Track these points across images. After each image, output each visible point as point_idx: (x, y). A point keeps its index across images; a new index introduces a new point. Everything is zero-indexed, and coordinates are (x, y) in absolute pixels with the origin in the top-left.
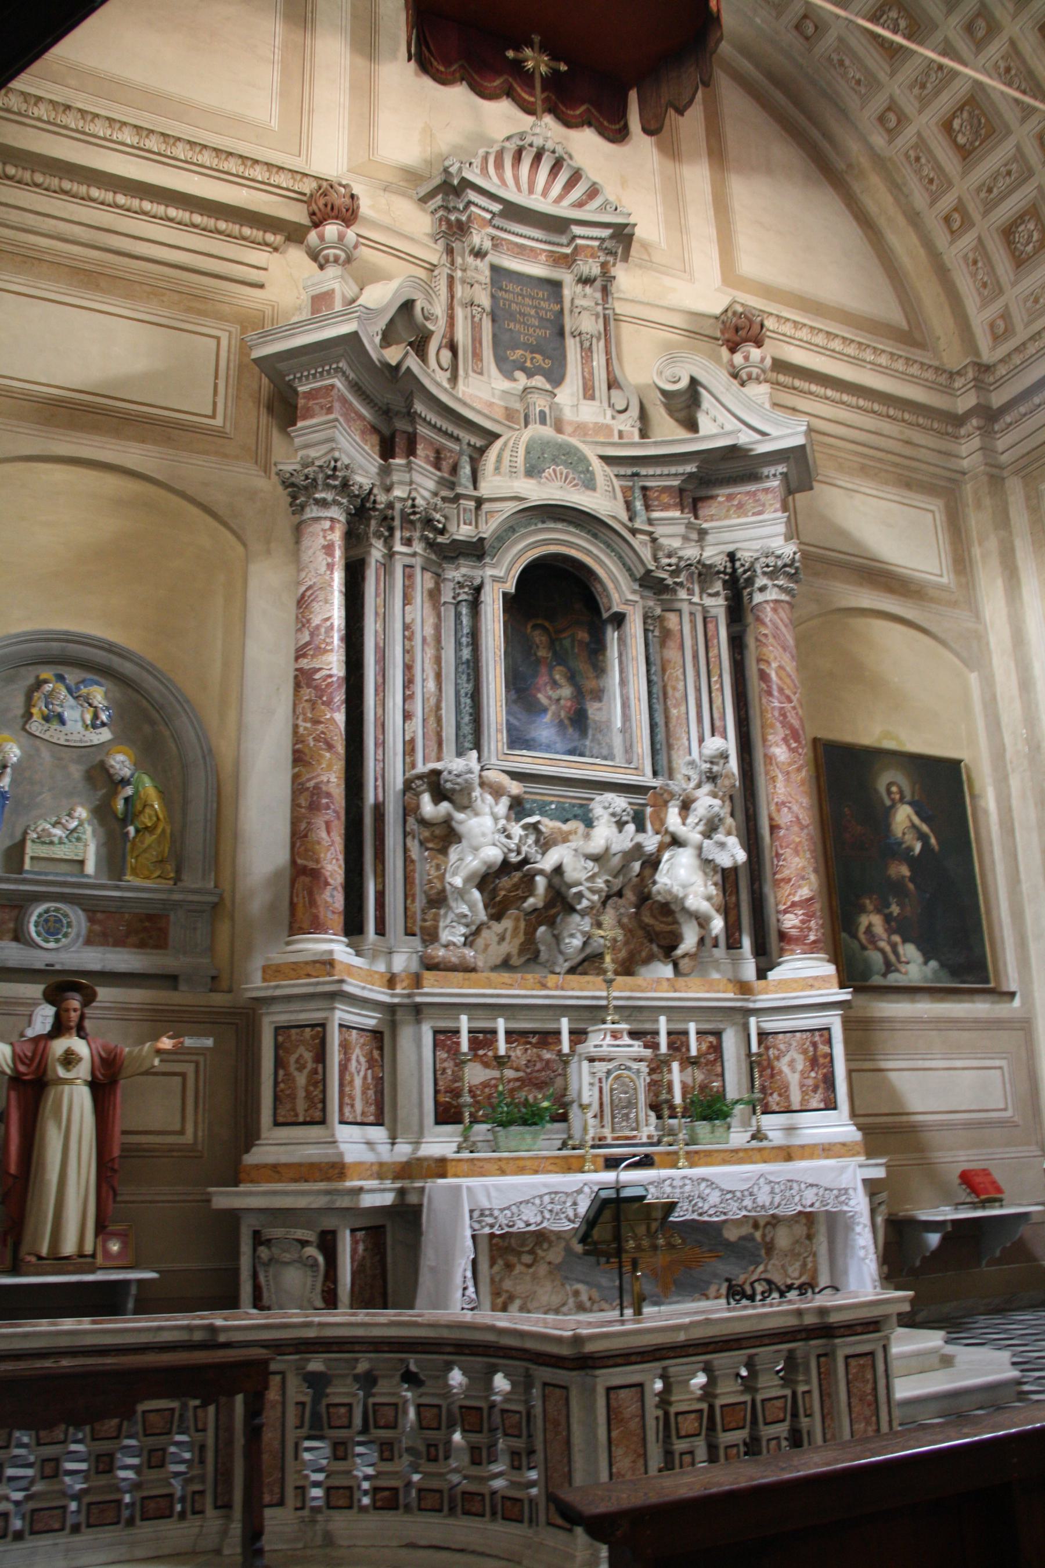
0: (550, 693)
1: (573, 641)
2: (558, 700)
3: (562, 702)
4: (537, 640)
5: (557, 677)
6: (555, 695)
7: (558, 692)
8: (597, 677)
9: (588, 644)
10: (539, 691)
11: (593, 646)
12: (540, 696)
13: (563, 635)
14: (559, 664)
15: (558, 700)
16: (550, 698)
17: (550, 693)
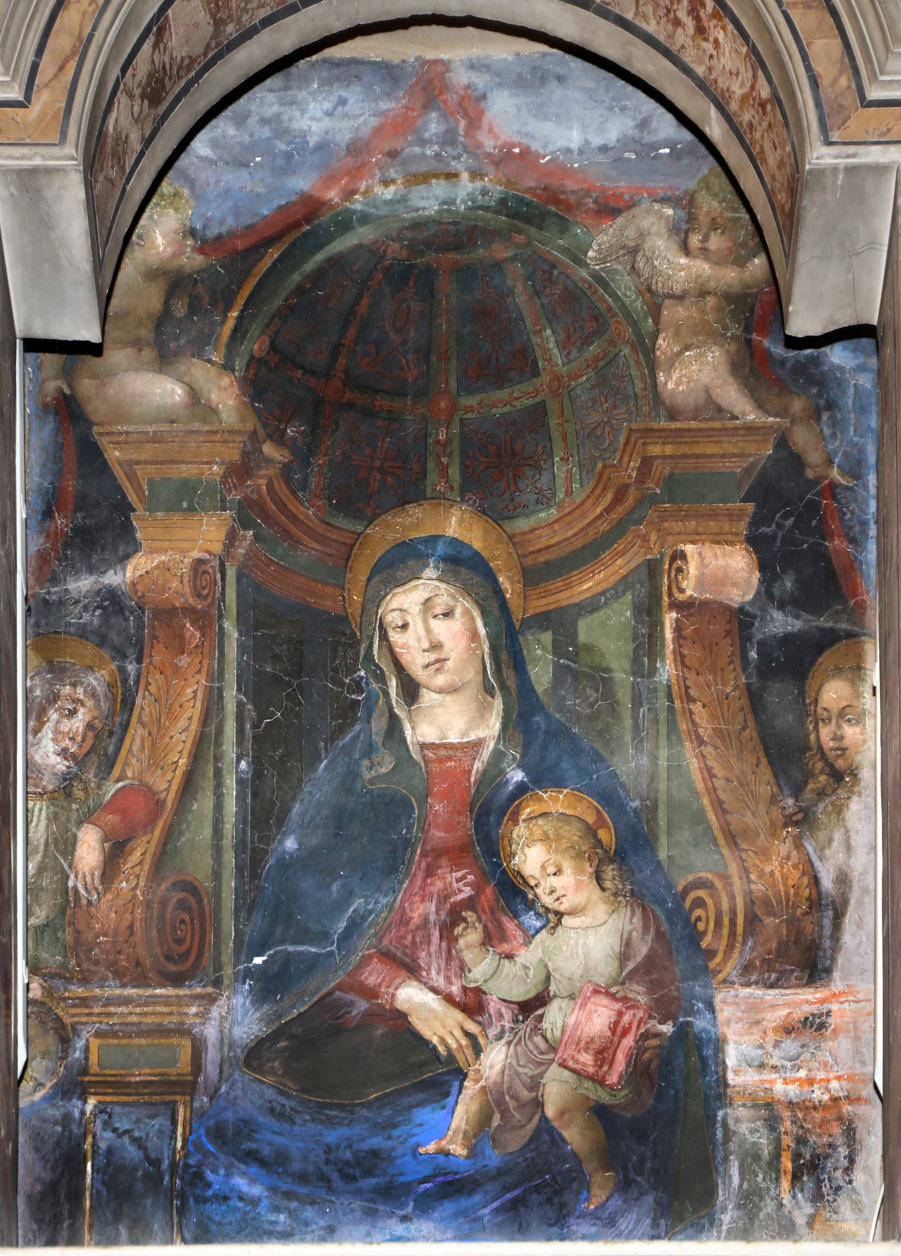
0: (481, 968)
1: (648, 612)
2: (531, 1007)
3: (554, 1017)
4: (411, 646)
5: (531, 859)
6: (505, 979)
7: (529, 955)
8: (803, 820)
9: (742, 620)
10: (412, 970)
11: (781, 623)
12: (412, 996)
13: (588, 585)
14: (542, 777)
15: (531, 1007)
16: (472, 1004)
17: (481, 968)
